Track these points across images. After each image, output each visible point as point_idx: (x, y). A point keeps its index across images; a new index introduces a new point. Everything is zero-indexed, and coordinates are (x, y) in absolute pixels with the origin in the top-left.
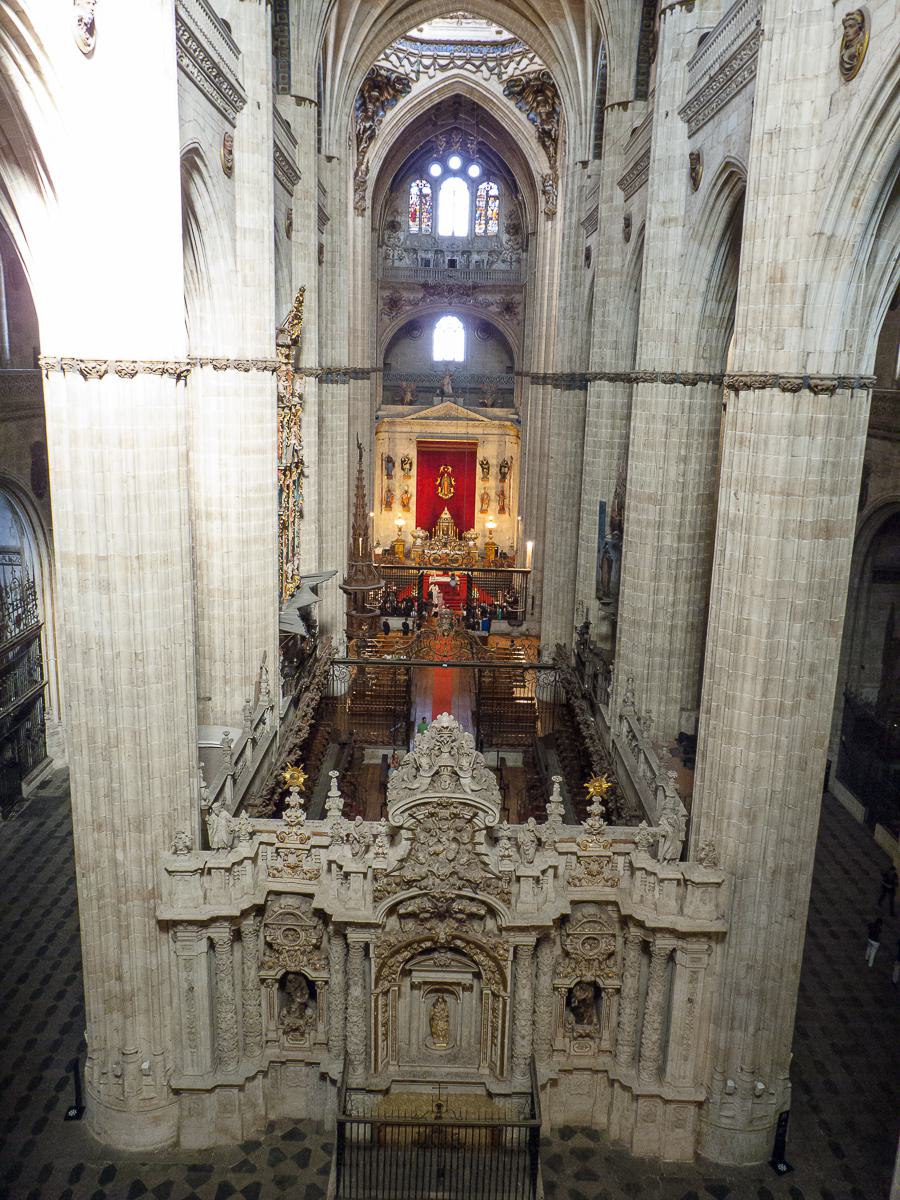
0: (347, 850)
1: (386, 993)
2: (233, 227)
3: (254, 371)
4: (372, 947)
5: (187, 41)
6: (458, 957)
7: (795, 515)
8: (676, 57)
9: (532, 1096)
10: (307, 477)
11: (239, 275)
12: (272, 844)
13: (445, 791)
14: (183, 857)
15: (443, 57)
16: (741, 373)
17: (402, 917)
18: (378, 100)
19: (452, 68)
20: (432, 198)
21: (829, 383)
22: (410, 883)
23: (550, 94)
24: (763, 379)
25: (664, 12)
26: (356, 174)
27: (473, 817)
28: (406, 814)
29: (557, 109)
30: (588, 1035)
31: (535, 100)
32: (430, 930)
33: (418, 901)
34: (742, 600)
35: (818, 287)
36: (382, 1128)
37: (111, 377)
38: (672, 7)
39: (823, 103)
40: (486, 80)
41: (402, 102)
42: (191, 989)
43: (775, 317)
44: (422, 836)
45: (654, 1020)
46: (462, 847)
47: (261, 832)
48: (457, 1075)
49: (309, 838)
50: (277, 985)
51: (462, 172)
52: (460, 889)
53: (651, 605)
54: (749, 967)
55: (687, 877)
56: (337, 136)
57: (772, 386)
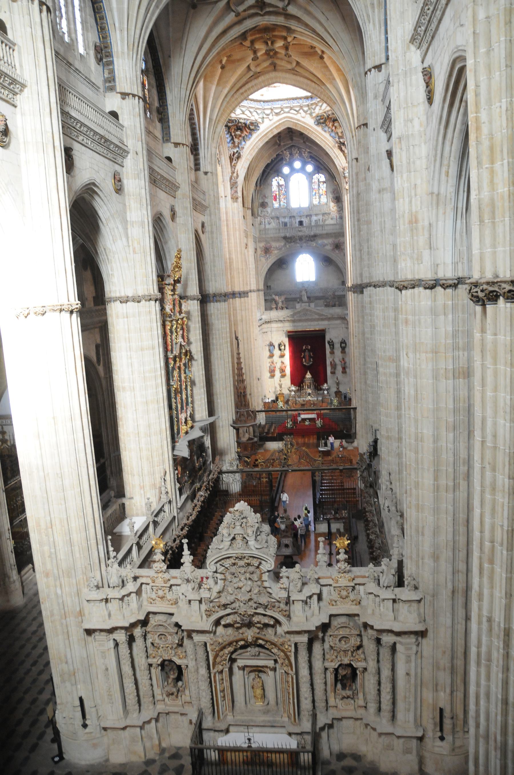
0: (190, 586)
1: (221, 672)
2: (125, 222)
3: (143, 302)
4: (208, 645)
5: (80, 127)
6: (264, 650)
7: (442, 365)
8: (376, 97)
9: (316, 736)
10: (196, 360)
11: (131, 248)
12: (148, 584)
13: (238, 549)
14: (94, 592)
15: (276, 108)
17: (226, 626)
18: (240, 136)
20: (285, 187)
21: (451, 282)
22: (225, 606)
24: (412, 282)
26: (231, 179)
28: (218, 564)
30: (348, 697)
31: (333, 125)
32: (242, 634)
33: (231, 616)
34: (416, 421)
36: (225, 753)
37: (32, 316)
38: (370, 70)
39: (424, 118)
42: (107, 669)
44: (229, 576)
45: (386, 688)
46: (255, 583)
47: (142, 577)
48: (269, 721)
49: (169, 580)
50: (160, 668)
51: (303, 170)
52: (255, 609)
53: (396, 425)
54: (444, 652)
56: (209, 160)
57: (419, 286)
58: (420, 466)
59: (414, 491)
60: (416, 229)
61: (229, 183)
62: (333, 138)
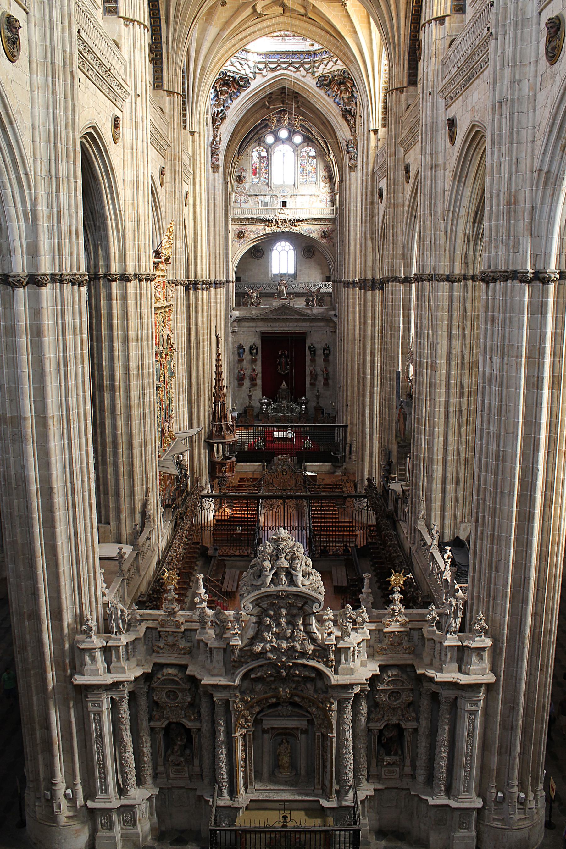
13: (284, 586)
16: (489, 270)
19: (279, 70)
20: (268, 159)
23: (349, 85)
24: (506, 274)
25: (424, 25)
27: (303, 605)
29: (355, 95)
31: (338, 89)
35: (541, 207)
38: (429, 22)
40: (303, 77)
41: (243, 94)
43: (512, 229)
55: (465, 644)
57: (513, 278)
58: (499, 490)
59: (488, 519)
60: (515, 212)
61: (210, 148)
62: (338, 104)
